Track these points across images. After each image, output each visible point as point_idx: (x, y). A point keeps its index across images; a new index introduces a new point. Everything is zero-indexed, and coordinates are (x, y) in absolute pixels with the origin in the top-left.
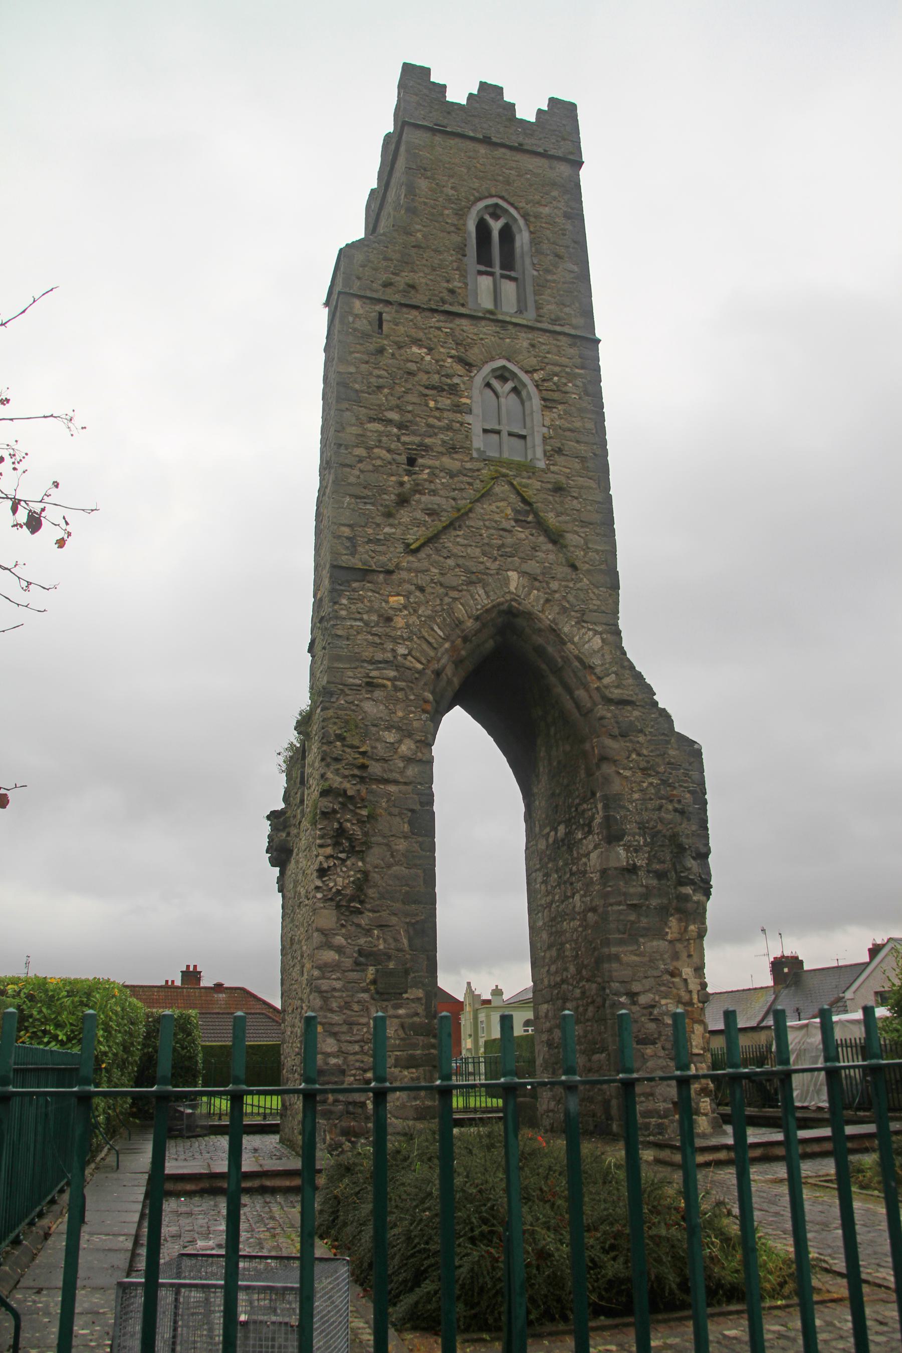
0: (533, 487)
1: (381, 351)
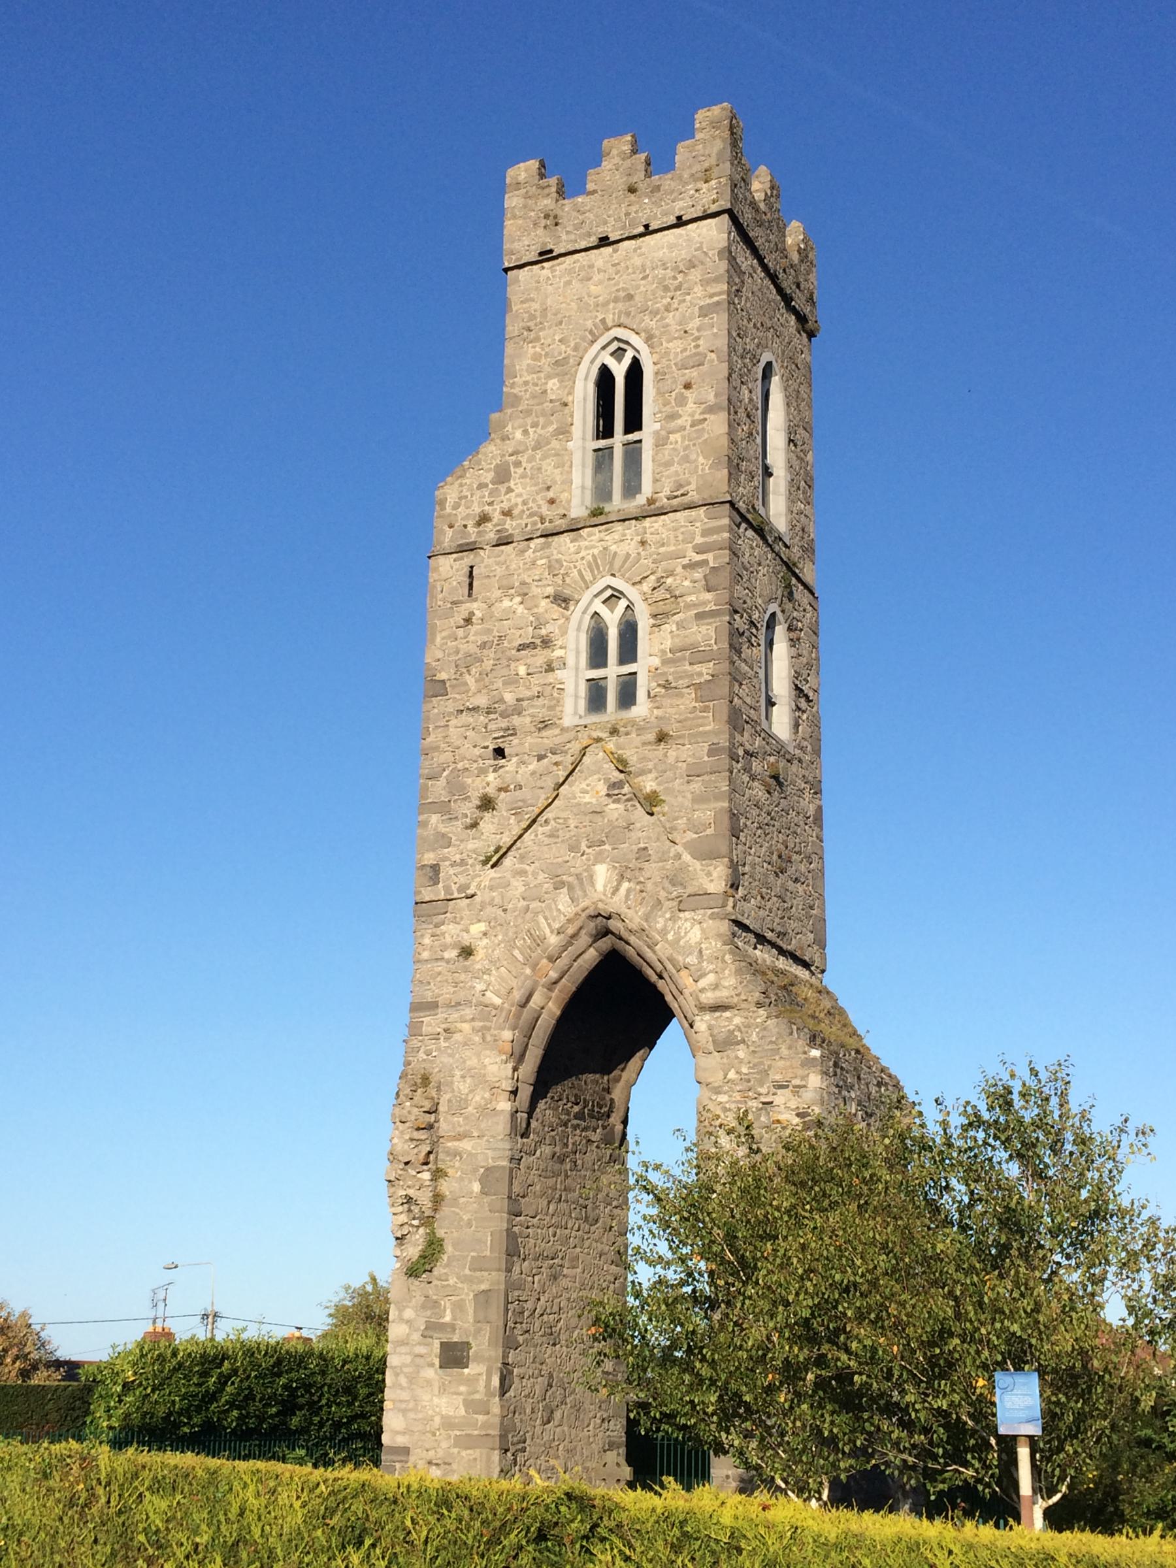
1: (468, 621)
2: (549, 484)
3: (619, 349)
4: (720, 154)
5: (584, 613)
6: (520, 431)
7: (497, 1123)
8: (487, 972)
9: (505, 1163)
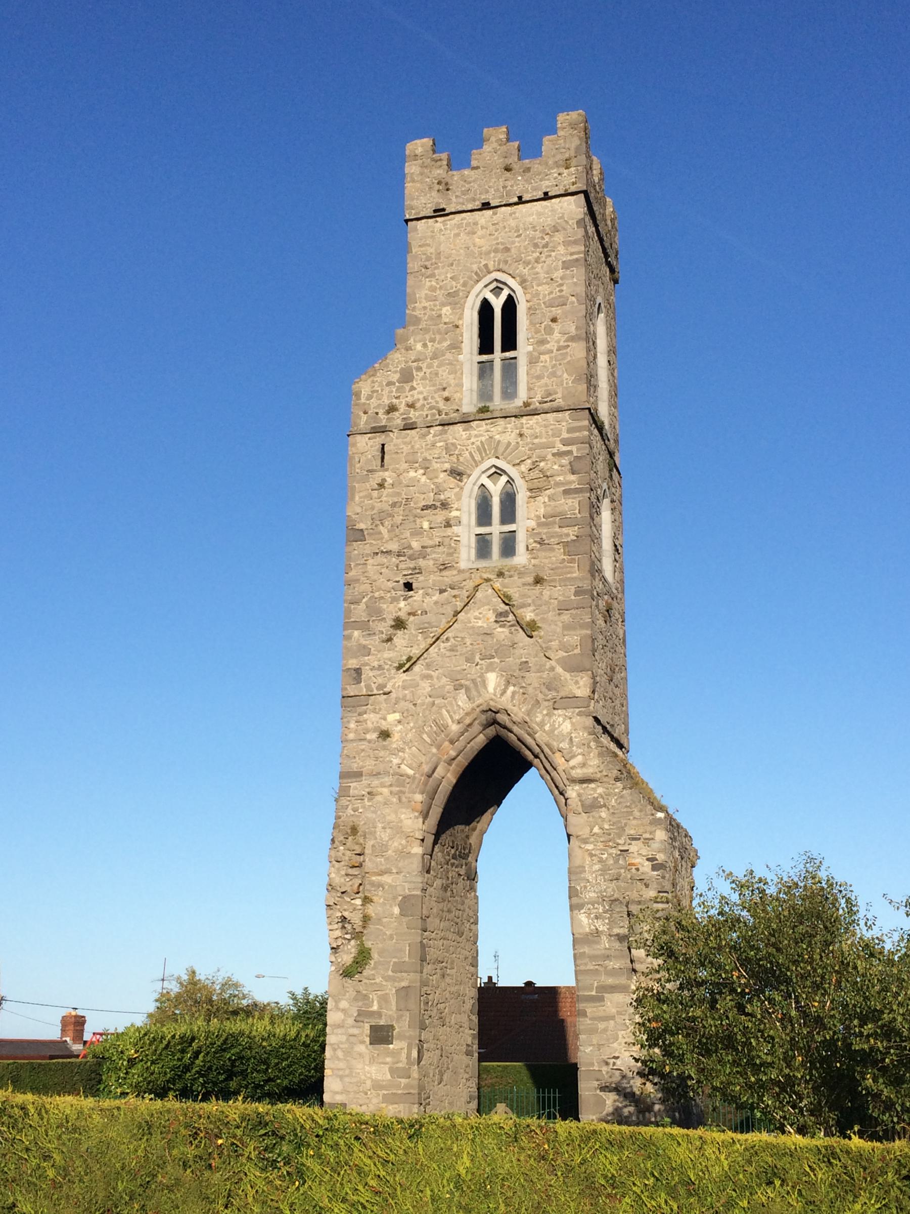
1: (381, 485)
2: (445, 386)
3: (497, 287)
4: (577, 149)
5: (474, 484)
6: (421, 344)
7: (412, 863)
8: (402, 750)
9: (419, 893)
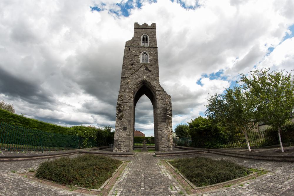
0: (147, 65)
